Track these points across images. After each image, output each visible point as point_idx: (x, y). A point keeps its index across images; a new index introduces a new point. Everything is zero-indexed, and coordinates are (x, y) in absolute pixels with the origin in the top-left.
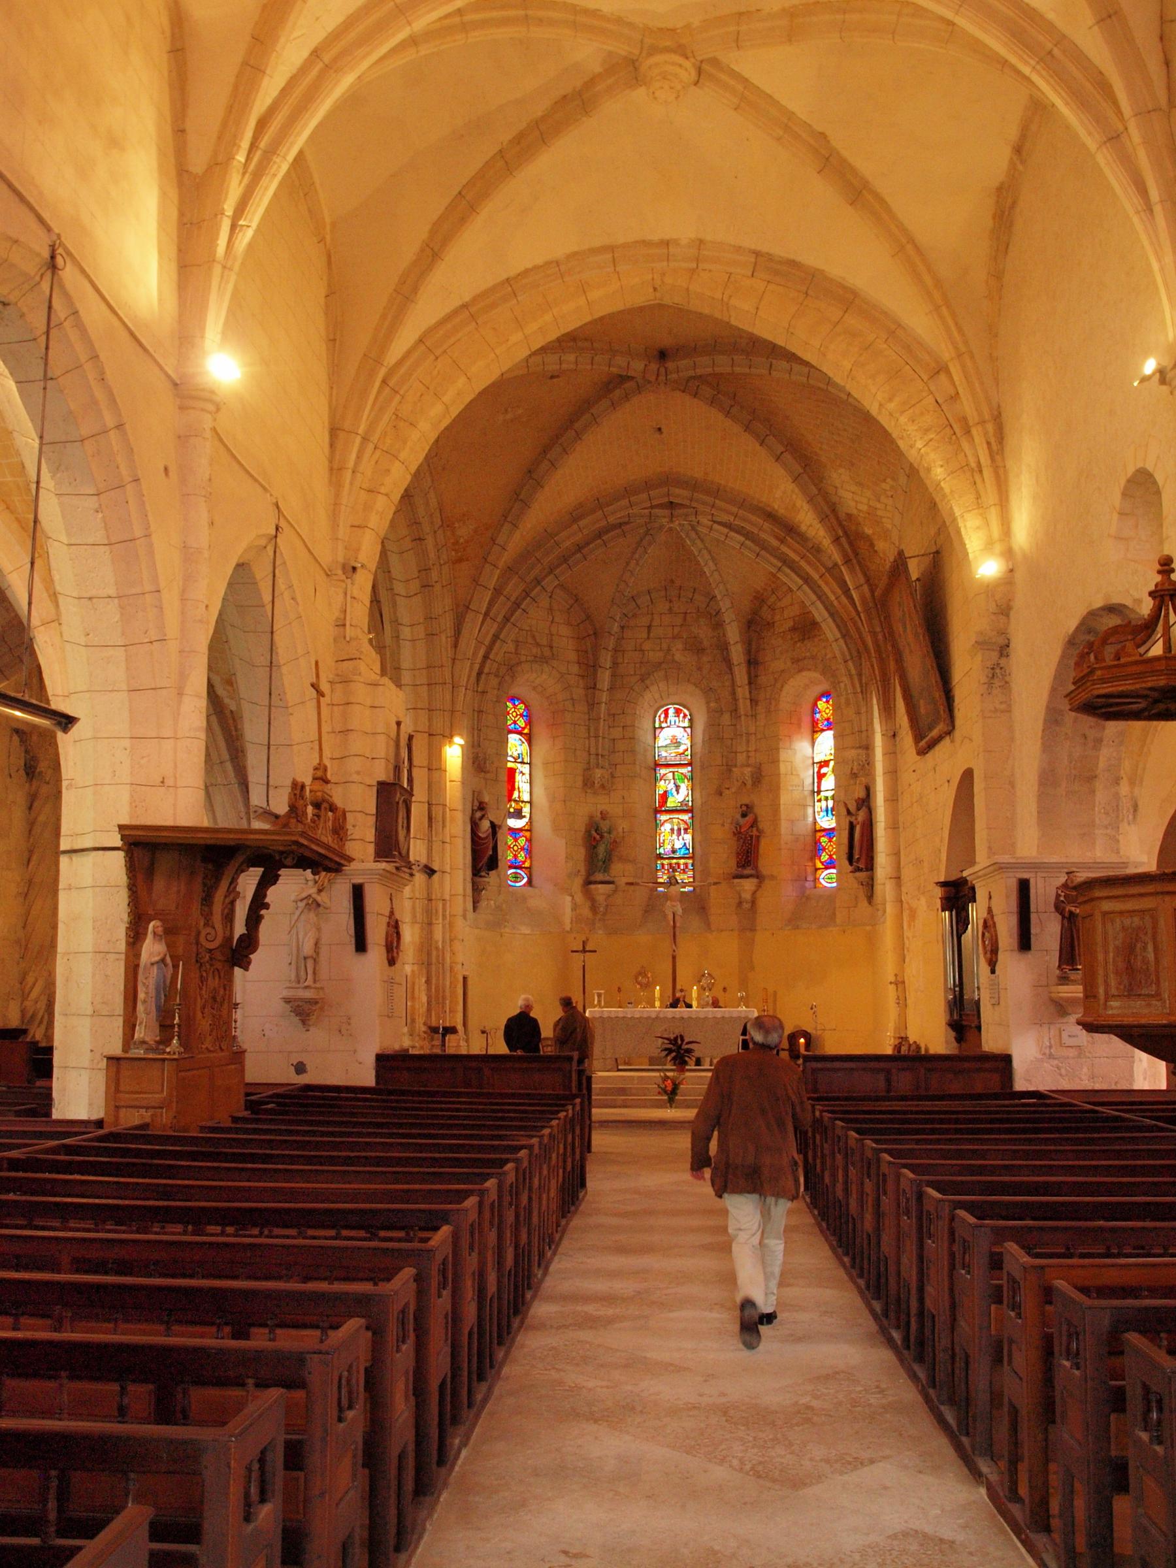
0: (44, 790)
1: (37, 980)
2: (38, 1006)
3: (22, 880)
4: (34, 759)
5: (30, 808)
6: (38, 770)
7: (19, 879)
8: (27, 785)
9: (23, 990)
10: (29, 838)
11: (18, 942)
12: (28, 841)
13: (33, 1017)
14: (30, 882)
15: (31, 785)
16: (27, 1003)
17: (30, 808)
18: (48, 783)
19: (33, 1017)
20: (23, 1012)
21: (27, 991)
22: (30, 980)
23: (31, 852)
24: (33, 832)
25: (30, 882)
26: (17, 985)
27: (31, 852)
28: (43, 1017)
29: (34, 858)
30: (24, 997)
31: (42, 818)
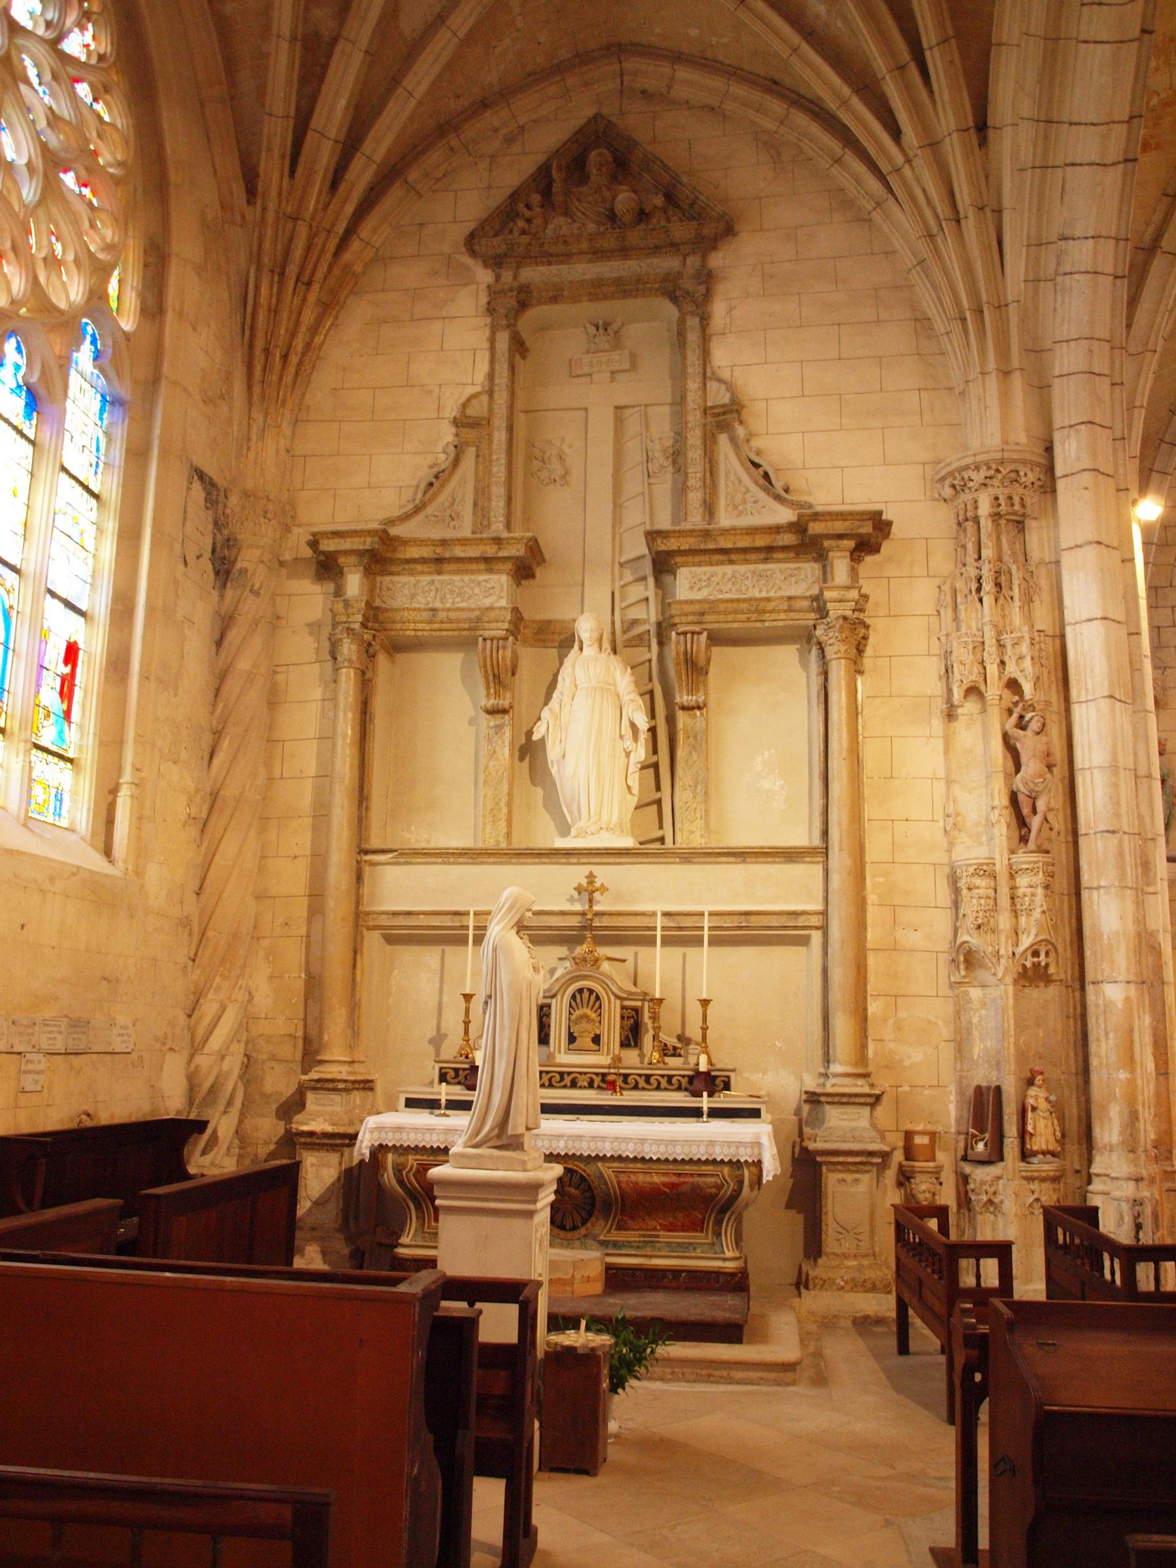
0: (250, 607)
1: (223, 1009)
2: (226, 1066)
3: (197, 790)
4: (230, 542)
5: (219, 643)
6: (238, 565)
7: (191, 786)
8: (215, 593)
9: (192, 1032)
10: (214, 705)
11: (185, 922)
12: (212, 713)
13: (213, 1091)
14: (214, 796)
15: (222, 597)
16: (202, 1060)
17: (219, 643)
18: (256, 593)
19: (213, 1091)
20: (192, 1081)
21: (201, 1032)
22: (209, 1008)
23: (218, 735)
24: (224, 694)
25: (214, 796)
26: (182, 1018)
27: (218, 735)
28: (234, 1089)
29: (225, 743)
30: (196, 1047)
31: (243, 664)
